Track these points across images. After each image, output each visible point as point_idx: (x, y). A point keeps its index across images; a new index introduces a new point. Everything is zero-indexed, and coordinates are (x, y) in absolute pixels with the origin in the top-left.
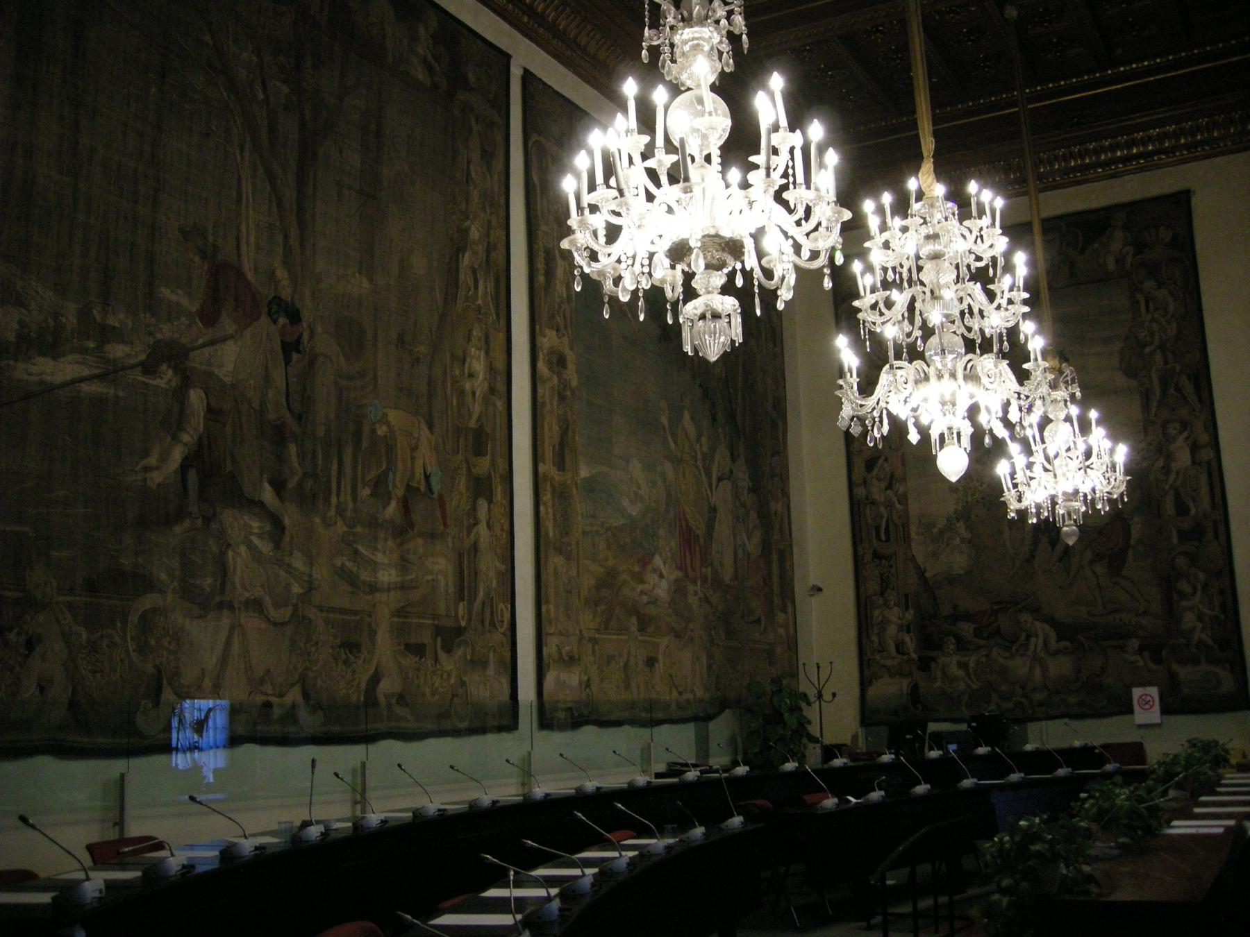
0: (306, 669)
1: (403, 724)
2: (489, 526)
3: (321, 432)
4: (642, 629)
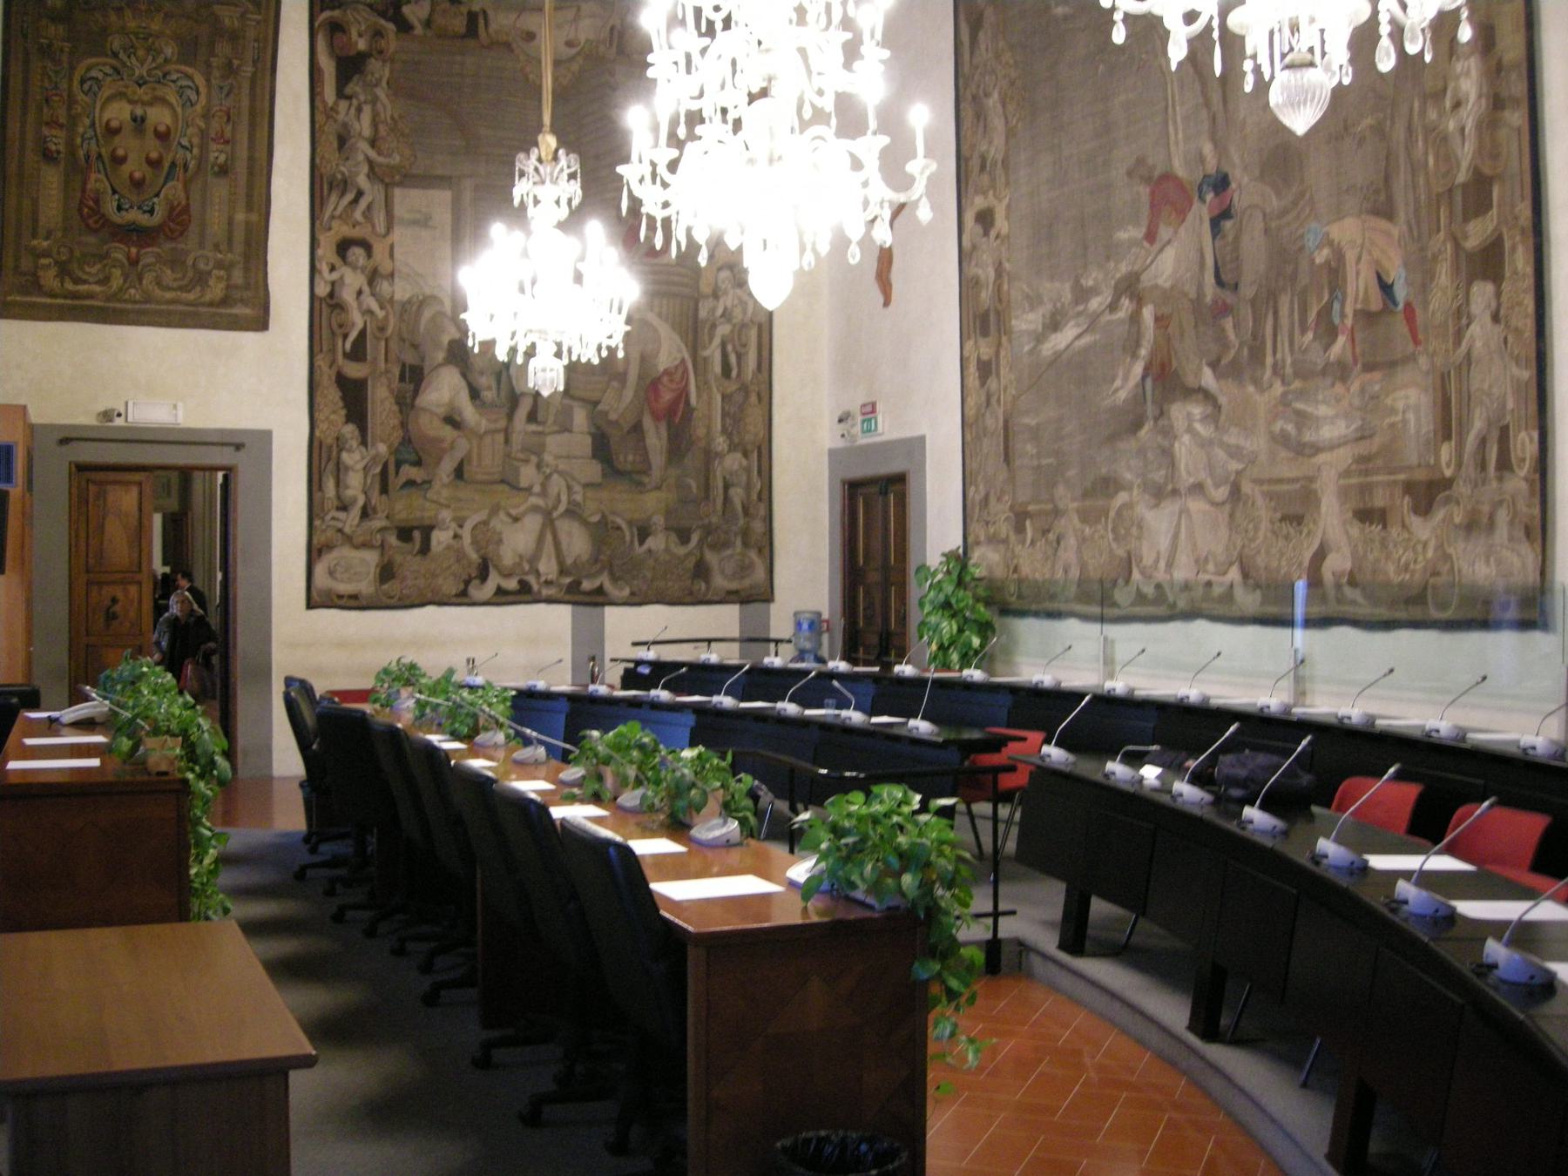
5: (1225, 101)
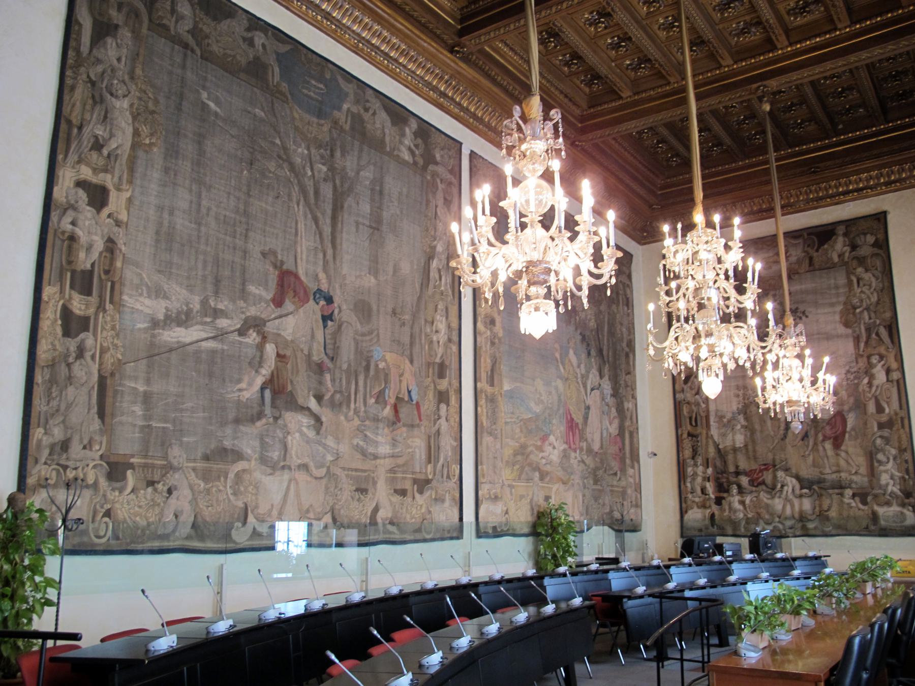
0: (335, 503)
1: (392, 536)
2: (447, 420)
3: (345, 366)
4: (542, 479)
5: (334, 258)
